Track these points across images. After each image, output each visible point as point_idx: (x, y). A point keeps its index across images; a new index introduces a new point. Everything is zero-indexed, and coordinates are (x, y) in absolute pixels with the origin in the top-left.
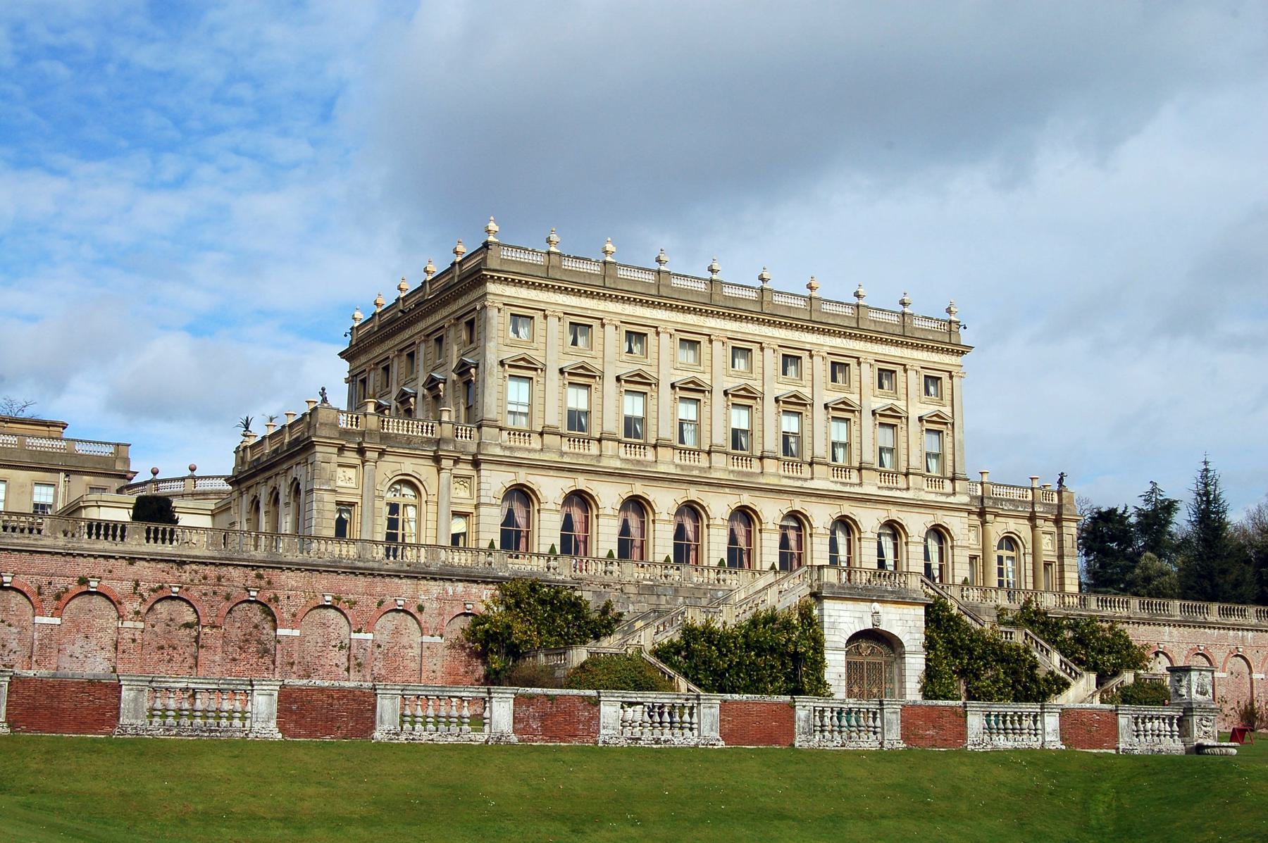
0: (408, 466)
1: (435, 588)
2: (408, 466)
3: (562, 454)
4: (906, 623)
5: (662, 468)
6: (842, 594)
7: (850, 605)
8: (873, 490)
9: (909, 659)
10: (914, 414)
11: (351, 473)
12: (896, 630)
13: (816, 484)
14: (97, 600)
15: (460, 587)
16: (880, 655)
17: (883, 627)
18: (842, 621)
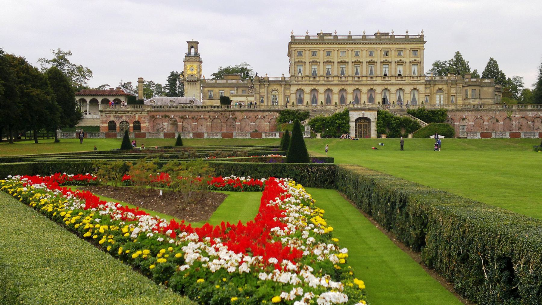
0: (275, 87)
1: (267, 113)
2: (275, 87)
3: (310, 81)
4: (372, 116)
5: (335, 82)
6: (353, 110)
7: (356, 112)
8: (394, 82)
9: (372, 123)
10: (408, 61)
11: (263, 89)
12: (369, 117)
13: (377, 82)
14: (203, 120)
15: (272, 113)
16: (363, 122)
17: (365, 116)
18: (354, 116)
